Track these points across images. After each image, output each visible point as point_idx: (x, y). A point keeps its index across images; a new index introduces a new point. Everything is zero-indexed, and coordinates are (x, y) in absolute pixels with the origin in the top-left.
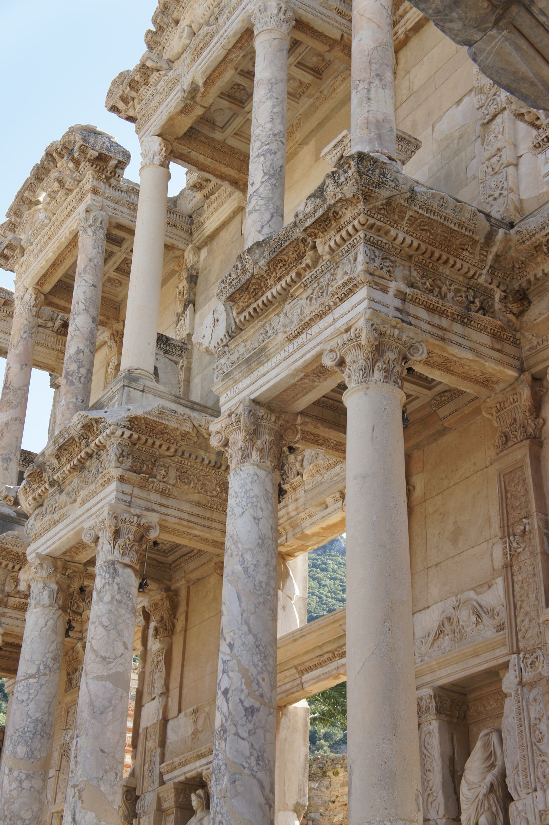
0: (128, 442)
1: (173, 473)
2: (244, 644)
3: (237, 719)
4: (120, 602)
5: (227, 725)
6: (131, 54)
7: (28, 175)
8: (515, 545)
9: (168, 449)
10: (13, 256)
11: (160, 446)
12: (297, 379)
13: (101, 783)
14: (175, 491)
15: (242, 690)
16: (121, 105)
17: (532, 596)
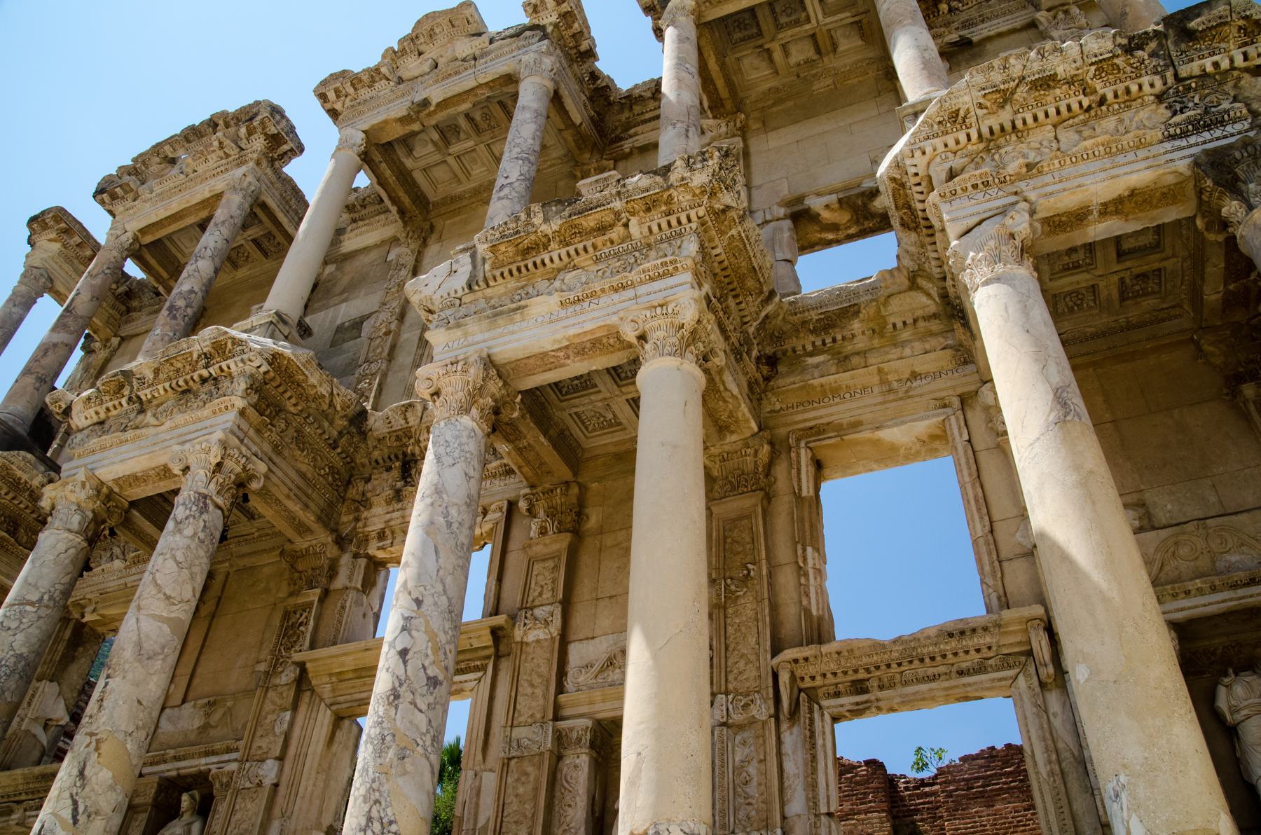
0: (260, 377)
1: (291, 432)
2: (435, 604)
3: (416, 686)
4: (202, 542)
5: (402, 690)
6: (364, 58)
7: (178, 132)
8: (733, 588)
9: (295, 405)
10: (123, 198)
11: (290, 398)
12: (556, 346)
13: (129, 739)
14: (286, 453)
15: (427, 655)
16: (331, 95)
17: (752, 640)
